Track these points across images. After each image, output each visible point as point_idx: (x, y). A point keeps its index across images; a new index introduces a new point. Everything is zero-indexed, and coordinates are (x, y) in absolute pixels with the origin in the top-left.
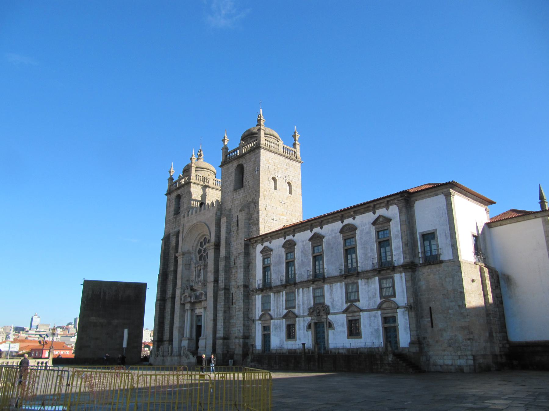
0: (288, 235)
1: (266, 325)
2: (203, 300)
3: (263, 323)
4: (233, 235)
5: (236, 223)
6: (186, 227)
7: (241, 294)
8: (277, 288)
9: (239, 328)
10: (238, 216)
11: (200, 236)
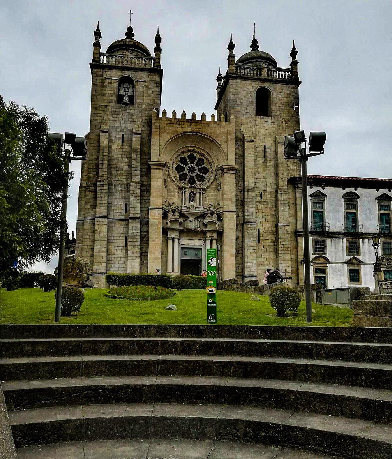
0: (349, 187)
1: (320, 268)
2: (209, 231)
3: (315, 265)
4: (259, 166)
5: (263, 154)
6: (167, 131)
7: (286, 232)
8: (335, 234)
9: (284, 268)
10: (265, 146)
11: (184, 150)
